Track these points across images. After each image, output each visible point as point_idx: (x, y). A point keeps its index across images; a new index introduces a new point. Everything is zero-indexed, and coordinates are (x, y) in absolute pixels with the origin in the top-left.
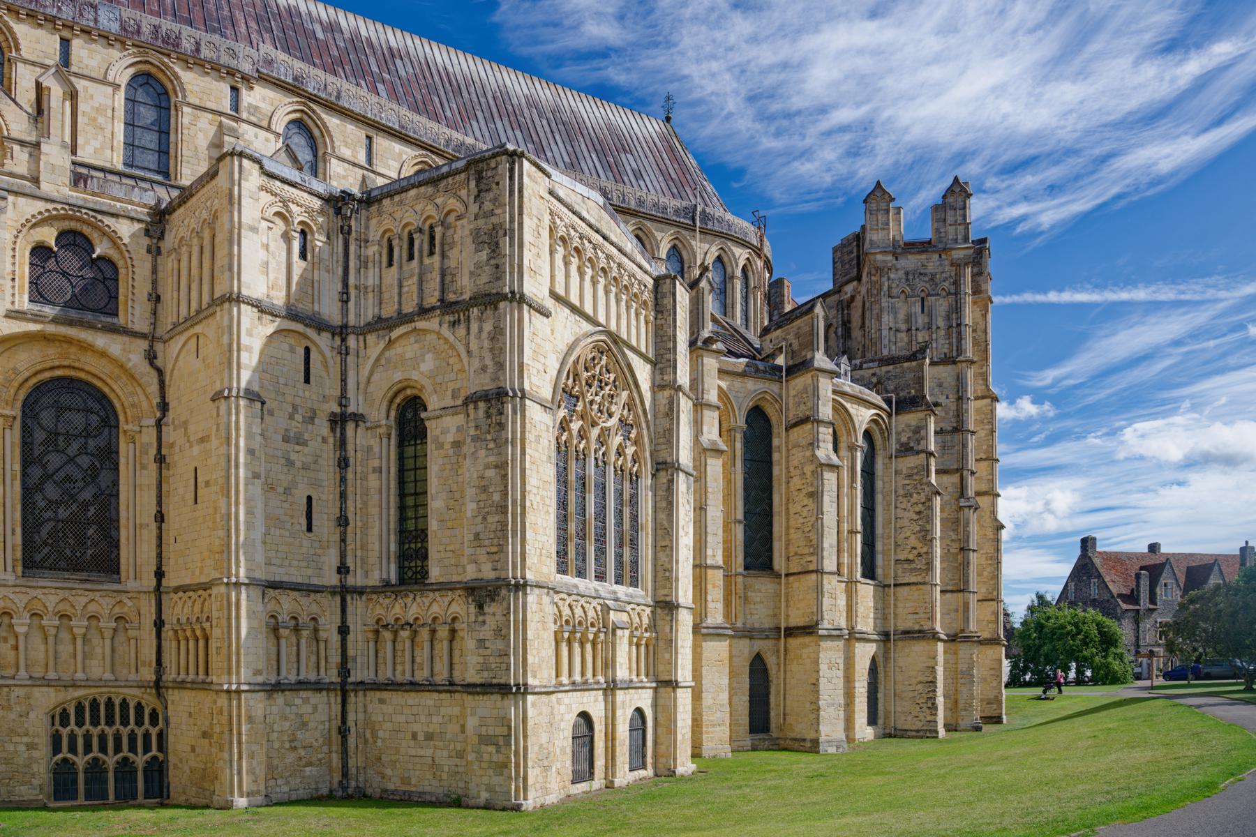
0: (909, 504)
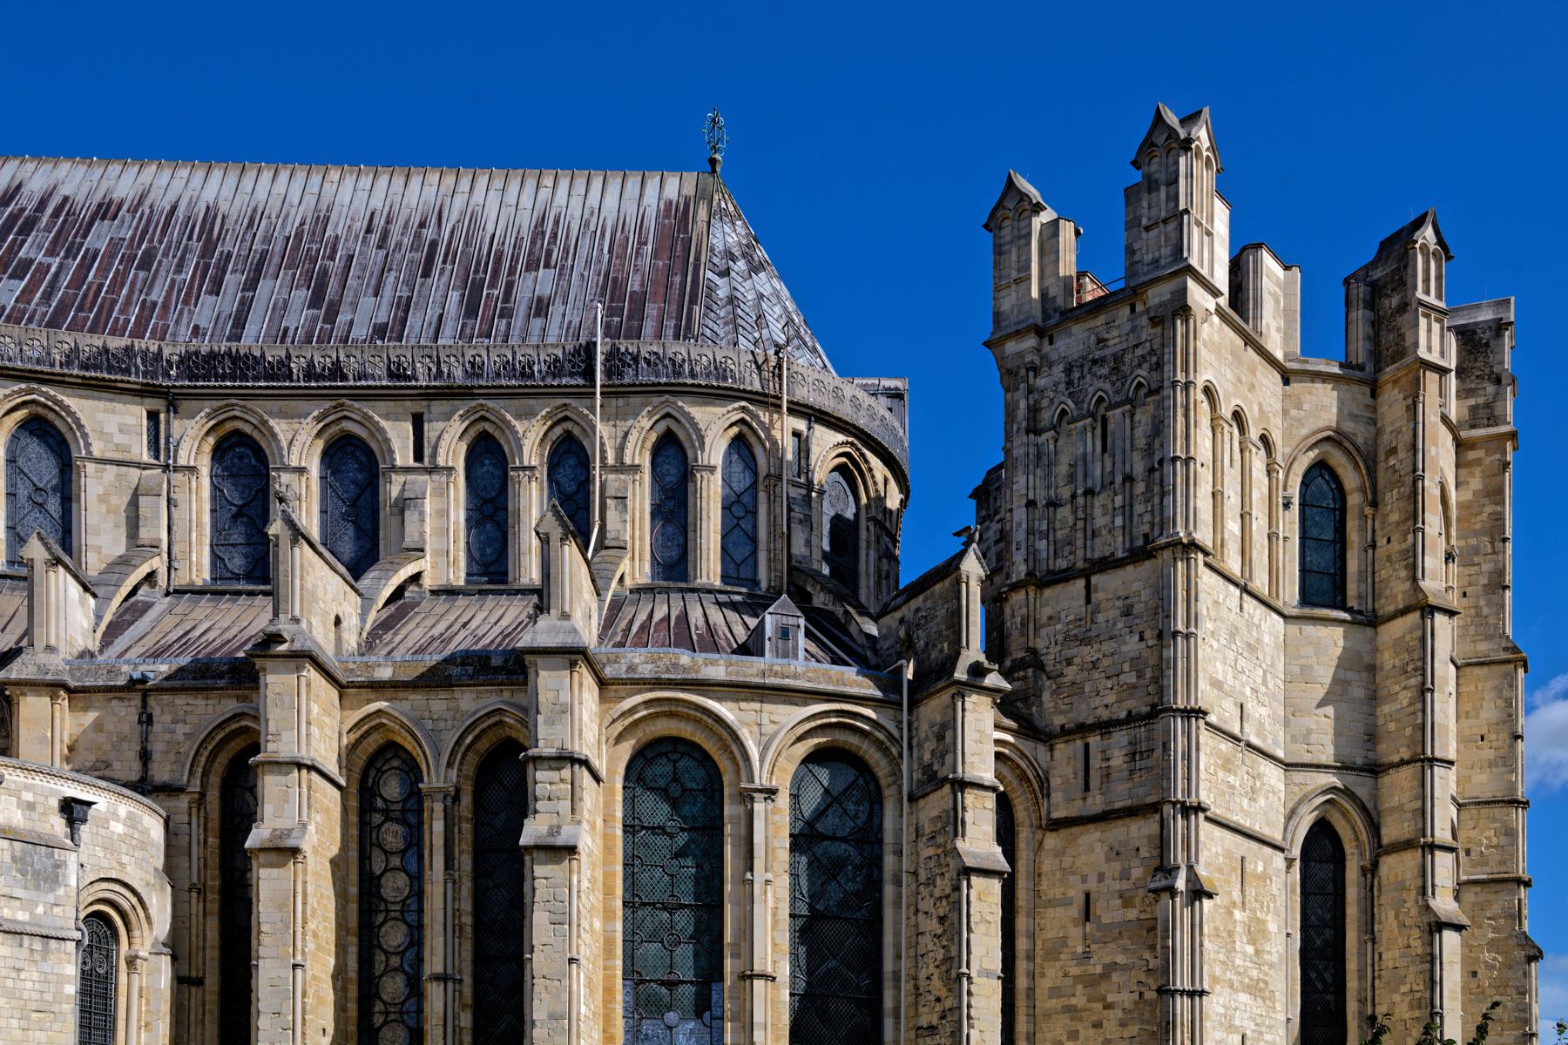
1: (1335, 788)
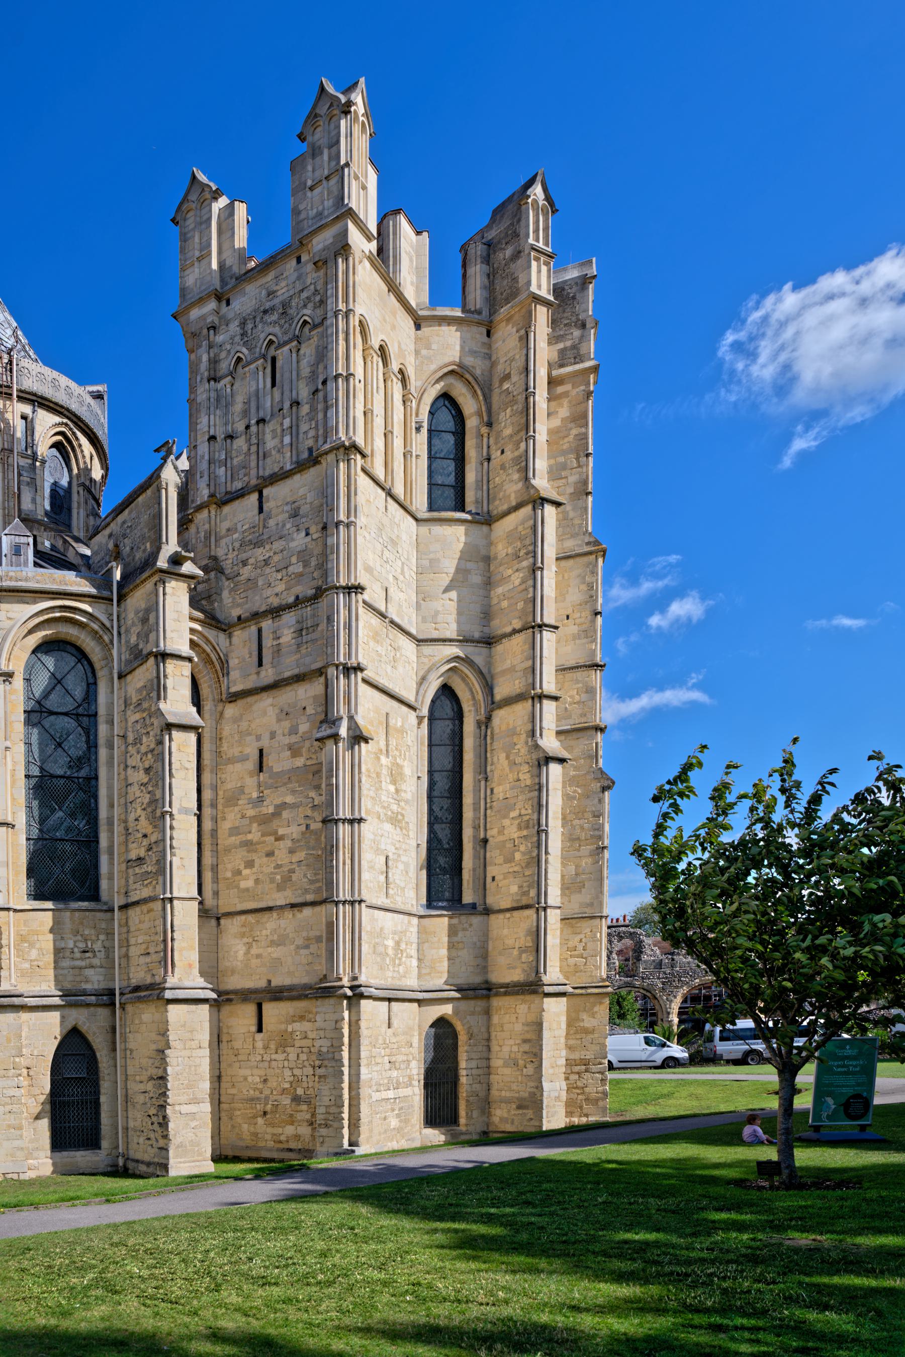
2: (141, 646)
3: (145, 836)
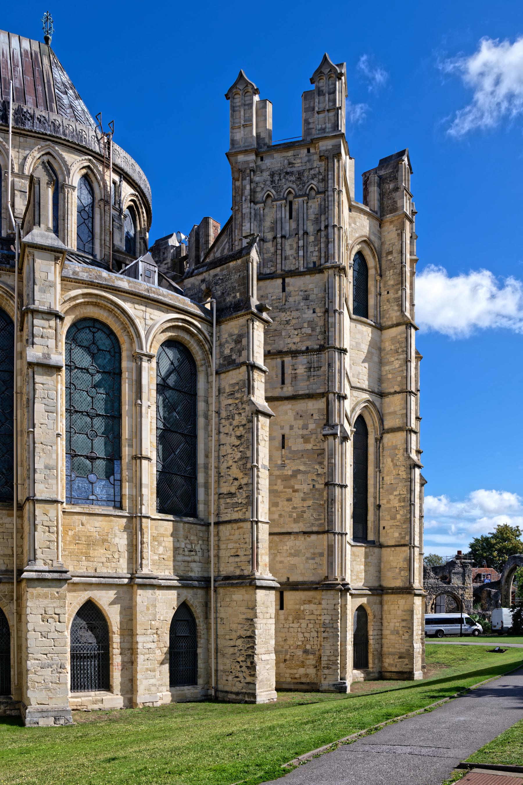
0: (231, 428)
1: (369, 400)
2: (234, 357)
3: (236, 479)
